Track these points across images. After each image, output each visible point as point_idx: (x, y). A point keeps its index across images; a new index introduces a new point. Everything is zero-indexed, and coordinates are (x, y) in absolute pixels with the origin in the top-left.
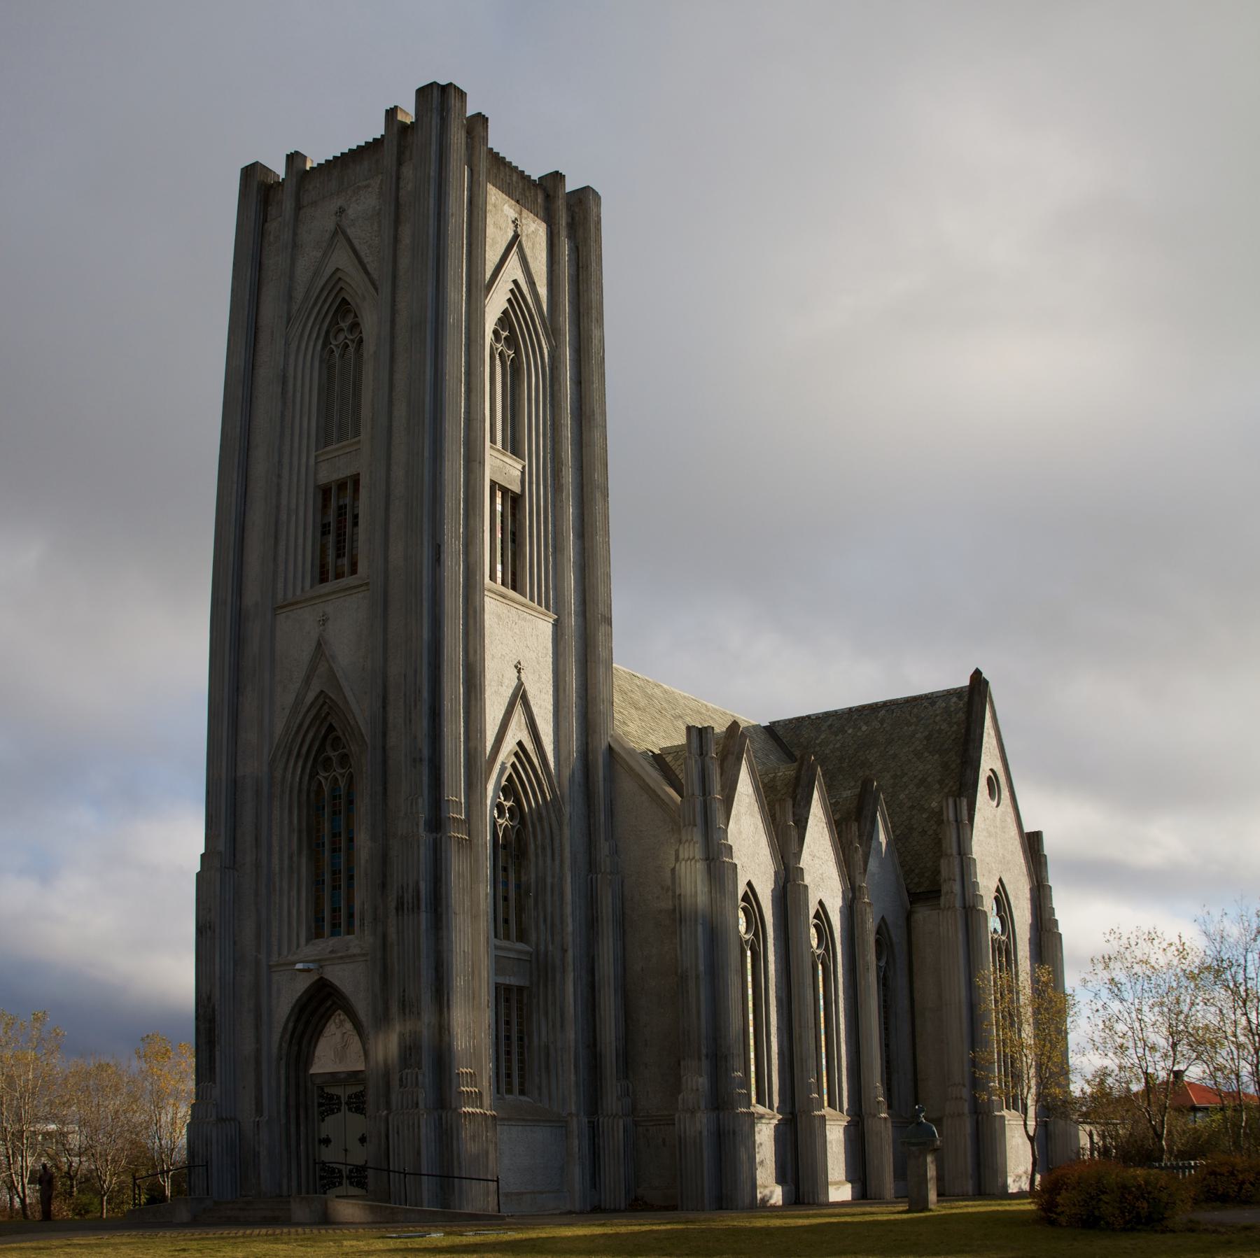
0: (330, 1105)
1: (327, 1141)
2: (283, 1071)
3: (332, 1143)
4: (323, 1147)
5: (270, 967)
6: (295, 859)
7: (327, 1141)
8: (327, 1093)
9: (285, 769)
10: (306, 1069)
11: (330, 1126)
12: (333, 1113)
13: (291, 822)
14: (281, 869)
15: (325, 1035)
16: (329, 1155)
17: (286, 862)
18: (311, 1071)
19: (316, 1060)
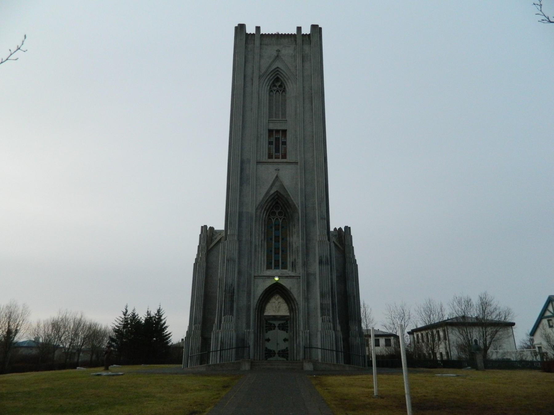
0: (271, 327)
1: (268, 340)
2: (257, 313)
3: (271, 341)
4: (266, 342)
5: (255, 276)
6: (263, 242)
7: (268, 340)
8: (269, 323)
9: (261, 212)
10: (263, 314)
11: (270, 334)
12: (271, 330)
13: (262, 230)
14: (259, 244)
15: (270, 302)
16: (270, 346)
17: (260, 242)
18: (266, 314)
19: (266, 311)
